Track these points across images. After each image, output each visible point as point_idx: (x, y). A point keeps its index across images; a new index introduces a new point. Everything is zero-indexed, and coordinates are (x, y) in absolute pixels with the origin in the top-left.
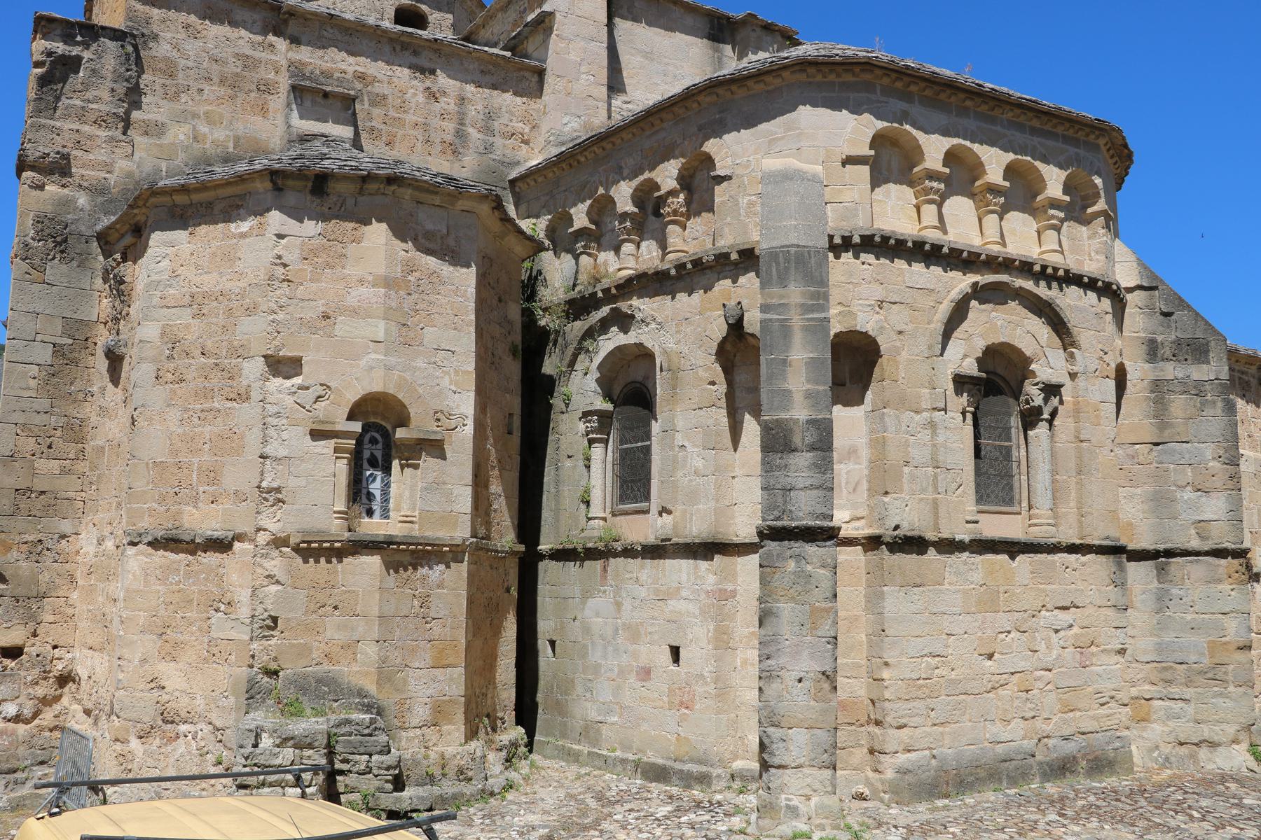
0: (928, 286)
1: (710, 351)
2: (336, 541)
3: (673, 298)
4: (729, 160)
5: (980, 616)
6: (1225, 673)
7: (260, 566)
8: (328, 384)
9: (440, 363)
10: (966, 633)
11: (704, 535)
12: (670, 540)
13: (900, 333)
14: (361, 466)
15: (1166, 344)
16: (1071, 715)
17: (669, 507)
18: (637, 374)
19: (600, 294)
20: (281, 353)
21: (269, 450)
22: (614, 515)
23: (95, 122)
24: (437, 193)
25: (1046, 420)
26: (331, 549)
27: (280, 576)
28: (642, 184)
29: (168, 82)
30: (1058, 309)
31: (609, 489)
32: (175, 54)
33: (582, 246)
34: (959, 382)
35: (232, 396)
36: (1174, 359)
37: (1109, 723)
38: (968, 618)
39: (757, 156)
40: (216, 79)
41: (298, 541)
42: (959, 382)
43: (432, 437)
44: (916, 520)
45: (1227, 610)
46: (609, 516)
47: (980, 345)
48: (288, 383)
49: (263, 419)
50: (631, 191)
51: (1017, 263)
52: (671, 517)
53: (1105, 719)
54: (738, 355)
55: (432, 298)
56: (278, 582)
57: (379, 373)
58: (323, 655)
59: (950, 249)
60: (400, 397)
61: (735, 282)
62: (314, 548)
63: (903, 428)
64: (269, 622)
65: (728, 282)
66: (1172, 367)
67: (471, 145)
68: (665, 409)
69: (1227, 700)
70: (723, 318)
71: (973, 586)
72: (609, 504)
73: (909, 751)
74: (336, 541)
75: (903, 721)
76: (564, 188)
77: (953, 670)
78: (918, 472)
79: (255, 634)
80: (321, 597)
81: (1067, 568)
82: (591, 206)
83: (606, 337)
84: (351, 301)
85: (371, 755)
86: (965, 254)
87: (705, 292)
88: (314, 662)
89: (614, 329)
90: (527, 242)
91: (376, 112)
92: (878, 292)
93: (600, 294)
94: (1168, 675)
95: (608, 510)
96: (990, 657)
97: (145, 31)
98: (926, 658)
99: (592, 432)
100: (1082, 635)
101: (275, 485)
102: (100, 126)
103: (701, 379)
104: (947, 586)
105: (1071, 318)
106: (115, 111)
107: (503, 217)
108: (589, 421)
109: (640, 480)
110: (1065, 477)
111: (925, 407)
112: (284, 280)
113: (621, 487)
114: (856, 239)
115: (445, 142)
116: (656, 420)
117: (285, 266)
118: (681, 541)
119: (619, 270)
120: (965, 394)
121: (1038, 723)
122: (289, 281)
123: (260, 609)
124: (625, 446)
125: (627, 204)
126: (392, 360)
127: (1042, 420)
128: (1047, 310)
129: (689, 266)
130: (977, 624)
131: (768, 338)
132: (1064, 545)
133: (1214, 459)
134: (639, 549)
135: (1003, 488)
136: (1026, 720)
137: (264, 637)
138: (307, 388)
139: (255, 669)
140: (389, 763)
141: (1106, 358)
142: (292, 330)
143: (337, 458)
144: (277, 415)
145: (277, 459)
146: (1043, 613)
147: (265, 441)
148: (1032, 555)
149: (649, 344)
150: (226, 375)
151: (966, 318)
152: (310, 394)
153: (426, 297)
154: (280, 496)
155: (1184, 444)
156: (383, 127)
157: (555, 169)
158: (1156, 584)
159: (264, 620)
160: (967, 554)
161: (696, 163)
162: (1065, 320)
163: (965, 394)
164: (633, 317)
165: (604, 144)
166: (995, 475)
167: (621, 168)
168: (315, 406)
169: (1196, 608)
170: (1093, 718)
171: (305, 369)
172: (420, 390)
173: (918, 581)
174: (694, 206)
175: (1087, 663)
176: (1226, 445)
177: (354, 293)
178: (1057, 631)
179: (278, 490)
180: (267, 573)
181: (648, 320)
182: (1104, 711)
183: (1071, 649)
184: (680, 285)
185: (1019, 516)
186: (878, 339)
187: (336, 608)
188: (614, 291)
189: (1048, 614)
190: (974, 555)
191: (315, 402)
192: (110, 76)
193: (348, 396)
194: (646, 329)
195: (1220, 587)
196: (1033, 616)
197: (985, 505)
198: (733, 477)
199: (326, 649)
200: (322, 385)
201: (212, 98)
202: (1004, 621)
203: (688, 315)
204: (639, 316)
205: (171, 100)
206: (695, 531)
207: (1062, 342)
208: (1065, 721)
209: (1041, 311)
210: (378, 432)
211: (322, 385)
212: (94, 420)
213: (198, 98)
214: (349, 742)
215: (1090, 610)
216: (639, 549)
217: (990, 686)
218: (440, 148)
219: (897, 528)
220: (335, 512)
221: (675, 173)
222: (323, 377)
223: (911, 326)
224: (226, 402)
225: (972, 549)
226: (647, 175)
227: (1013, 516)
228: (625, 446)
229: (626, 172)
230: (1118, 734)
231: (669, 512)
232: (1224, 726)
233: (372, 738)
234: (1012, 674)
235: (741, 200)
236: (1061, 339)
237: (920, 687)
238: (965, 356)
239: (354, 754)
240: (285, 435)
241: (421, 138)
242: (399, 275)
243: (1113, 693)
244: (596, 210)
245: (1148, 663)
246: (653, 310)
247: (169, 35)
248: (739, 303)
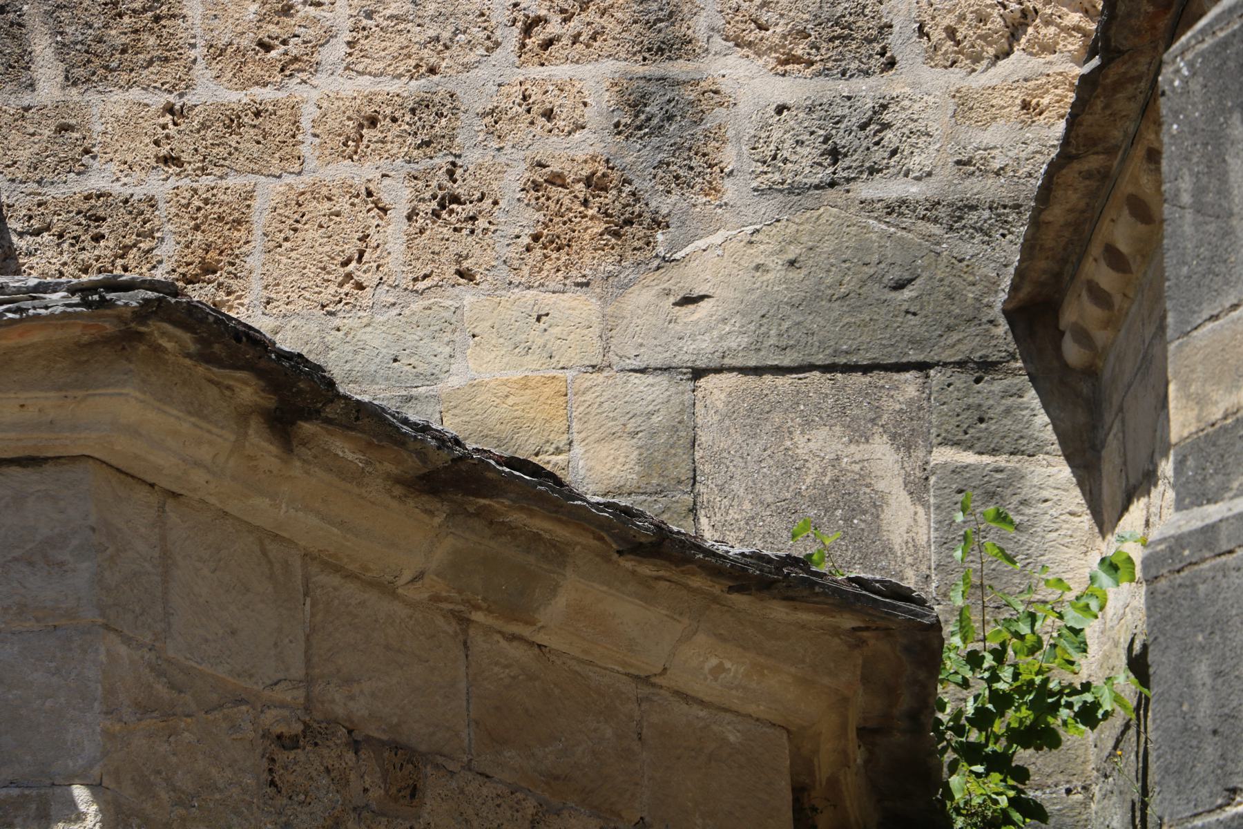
67: (729, 157)
107: (412, 465)
115: (557, 180)
131: (1202, 671)
156: (159, 185)
218: (528, 219)
241: (399, 195)
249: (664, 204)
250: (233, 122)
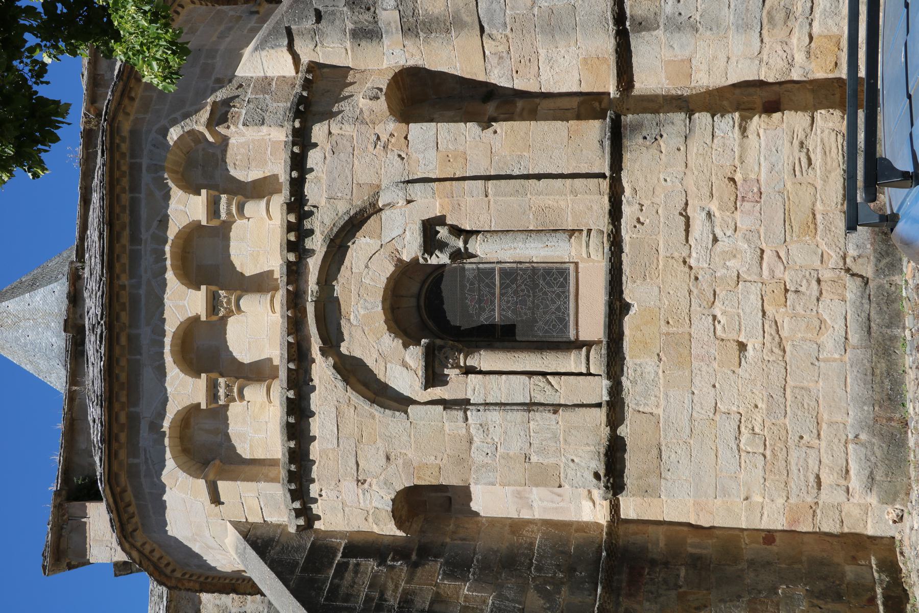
0: (334, 415)
5: (695, 364)
10: (714, 386)
13: (388, 458)
15: (355, 18)
16: (819, 217)
25: (466, 242)
30: (335, 230)
34: (433, 379)
36: (372, 9)
37: (834, 150)
38: (697, 381)
42: (433, 379)
44: (588, 448)
47: (390, 343)
51: (290, 288)
53: (829, 159)
59: (289, 389)
63: (488, 460)
66: (384, 13)
71: (660, 373)
73: (847, 471)
75: (812, 479)
77: (756, 406)
78: (536, 443)
81: (638, 220)
86: (292, 366)
92: (349, 485)
94: (779, 16)
96: (742, 347)
98: (742, 446)
100: (721, 199)
104: (660, 411)
105: (343, 209)
110: (531, 216)
111: (464, 431)
114: (297, 505)
120: (446, 371)
121: (826, 275)
127: (466, 249)
128: (338, 241)
130: (704, 368)
132: (611, 227)
135: (548, 284)
136: (821, 293)
141: (384, 138)
146: (692, 262)
148: (624, 278)
151: (360, 361)
158: (660, 33)
160: (624, 379)
162: (346, 218)
163: (446, 371)
166: (534, 296)
170: (825, 180)
173: (655, 452)
175: (756, 190)
178: (715, 240)
183: (738, 215)
185: (580, 265)
186: (399, 487)
189: (694, 254)
190: (625, 369)
196: (697, 279)
197: (568, 315)
202: (701, 327)
207: (372, 214)
208: (828, 229)
209: (340, 247)
215: (690, 182)
217: (776, 350)
219: (597, 476)
223: (380, 443)
225: (618, 373)
227: (580, 275)
234: (764, 313)
236: (369, 217)
237: (774, 455)
238: (405, 365)
243: (796, 143)
245: (762, 41)
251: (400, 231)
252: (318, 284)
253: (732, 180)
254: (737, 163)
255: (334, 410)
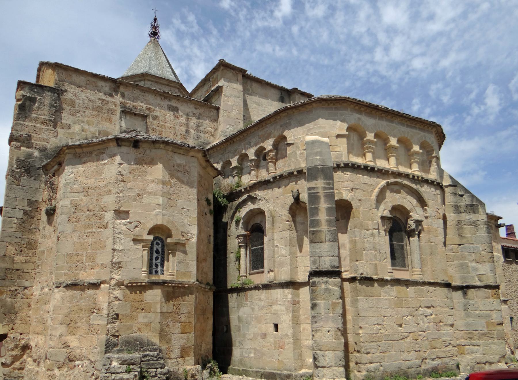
0: (370, 183)
1: (287, 209)
2: (143, 283)
3: (272, 190)
4: (293, 137)
5: (396, 309)
6: (493, 334)
7: (112, 293)
8: (140, 221)
9: (183, 214)
10: (391, 316)
11: (286, 279)
12: (273, 282)
13: (360, 200)
14: (153, 253)
16: (434, 350)
17: (272, 269)
18: (257, 220)
19: (243, 190)
20: (121, 209)
21: (116, 247)
22: (250, 274)
23: (42, 123)
24: (182, 149)
26: (141, 286)
27: (120, 297)
28: (258, 149)
29: (72, 108)
30: (420, 192)
31: (248, 265)
32: (74, 98)
33: (236, 173)
35: (100, 226)
37: (450, 354)
38: (391, 310)
39: (304, 135)
40: (91, 108)
41: (127, 282)
43: (181, 242)
44: (369, 271)
45: (492, 309)
46: (248, 275)
47: (390, 205)
48: (124, 221)
49: (114, 235)
50: (254, 151)
52: (273, 273)
53: (447, 352)
54: (297, 210)
55: (180, 189)
56: (119, 300)
57: (160, 217)
58: (137, 329)
60: (168, 226)
61: (296, 183)
62: (134, 286)
63: (363, 236)
64: (115, 316)
65: (294, 183)
68: (270, 232)
69: (495, 345)
70: (292, 197)
71: (392, 297)
72: (248, 270)
73: (372, 363)
74: (143, 283)
75: (368, 351)
76: (228, 152)
77: (387, 330)
78: (368, 253)
79: (109, 321)
80: (136, 305)
81: (428, 291)
82: (239, 158)
83: (246, 206)
84: (149, 189)
85: (157, 369)
86: (383, 171)
87: (285, 187)
88: (134, 332)
89: (249, 203)
90: (215, 171)
91: (155, 122)
92: (351, 185)
93: (243, 190)
94: (469, 336)
95: (248, 273)
96: (401, 326)
97: (62, 89)
98: (376, 326)
99: (241, 243)
100: (436, 318)
101: (118, 260)
102: (44, 124)
103: (283, 220)
104: (382, 297)
106: (50, 119)
108: (240, 239)
109: (259, 261)
111: (370, 228)
112: (122, 181)
113: (252, 263)
114: (342, 165)
116: (266, 236)
117: (122, 175)
118: (277, 282)
119: (250, 181)
121: (422, 353)
122: (124, 181)
123: (111, 311)
124: (254, 248)
125: (253, 157)
126: (165, 212)
129: (278, 177)
130: (395, 313)
133: (483, 250)
134: (261, 286)
136: (416, 351)
137: (113, 322)
138: (132, 223)
139: (109, 336)
140: (165, 372)
141: (439, 211)
142: (125, 200)
143: (144, 250)
144: (119, 233)
145: (119, 251)
146: (420, 309)
147: (114, 244)
149: (263, 208)
150: (98, 218)
152: (133, 225)
153: (178, 189)
154: (120, 265)
155: (471, 245)
157: (224, 145)
158: (463, 300)
159: (113, 315)
161: (280, 140)
164: (256, 198)
165: (243, 134)
167: (250, 143)
168: (134, 230)
169: (480, 309)
171: (131, 215)
172: (176, 224)
173: (371, 295)
174: (279, 156)
176: (487, 245)
177: (150, 186)
178: (426, 316)
179: (120, 263)
180: (115, 296)
181: (262, 199)
182: (447, 349)
183: (432, 324)
184: (274, 185)
186: (352, 202)
187: (143, 309)
188: (248, 189)
189: (422, 309)
191: (135, 228)
192: (48, 105)
193: (148, 226)
194: (261, 203)
195: (489, 300)
196: (417, 310)
198: (297, 257)
199: (139, 327)
200: (137, 221)
201: (89, 115)
202: (405, 311)
203: (278, 196)
204: (258, 198)
205: (73, 115)
206: (283, 278)
208: (432, 352)
210: (159, 240)
211: (137, 221)
212: (40, 240)
213: (84, 115)
214: (148, 364)
215: (438, 308)
216: (261, 286)
217: (401, 337)
219: (362, 274)
220: (143, 271)
221: (272, 143)
222: (138, 218)
223: (364, 198)
224: (98, 229)
226: (262, 144)
228: (254, 248)
229: (252, 144)
230: (453, 358)
231: (272, 271)
232: (494, 356)
233: (158, 362)
234: (410, 333)
235: (297, 152)
237: (374, 337)
238: (385, 210)
239: (150, 368)
240: (122, 241)
242: (167, 180)
243: (450, 342)
244: (240, 159)
245: (462, 331)
246: (264, 195)
247: (72, 90)
248: (298, 190)
249: (188, 138)
250: (162, 125)
251: (418, 213)
252: (405, 184)
253: (440, 322)
254: (445, 323)
255: (371, 183)
